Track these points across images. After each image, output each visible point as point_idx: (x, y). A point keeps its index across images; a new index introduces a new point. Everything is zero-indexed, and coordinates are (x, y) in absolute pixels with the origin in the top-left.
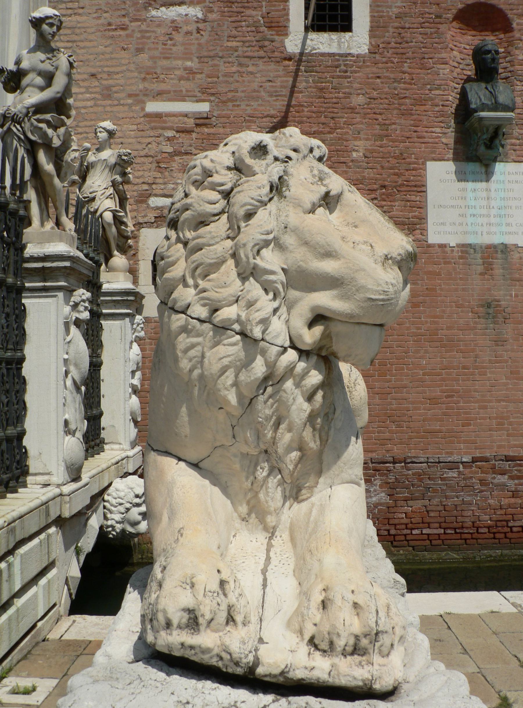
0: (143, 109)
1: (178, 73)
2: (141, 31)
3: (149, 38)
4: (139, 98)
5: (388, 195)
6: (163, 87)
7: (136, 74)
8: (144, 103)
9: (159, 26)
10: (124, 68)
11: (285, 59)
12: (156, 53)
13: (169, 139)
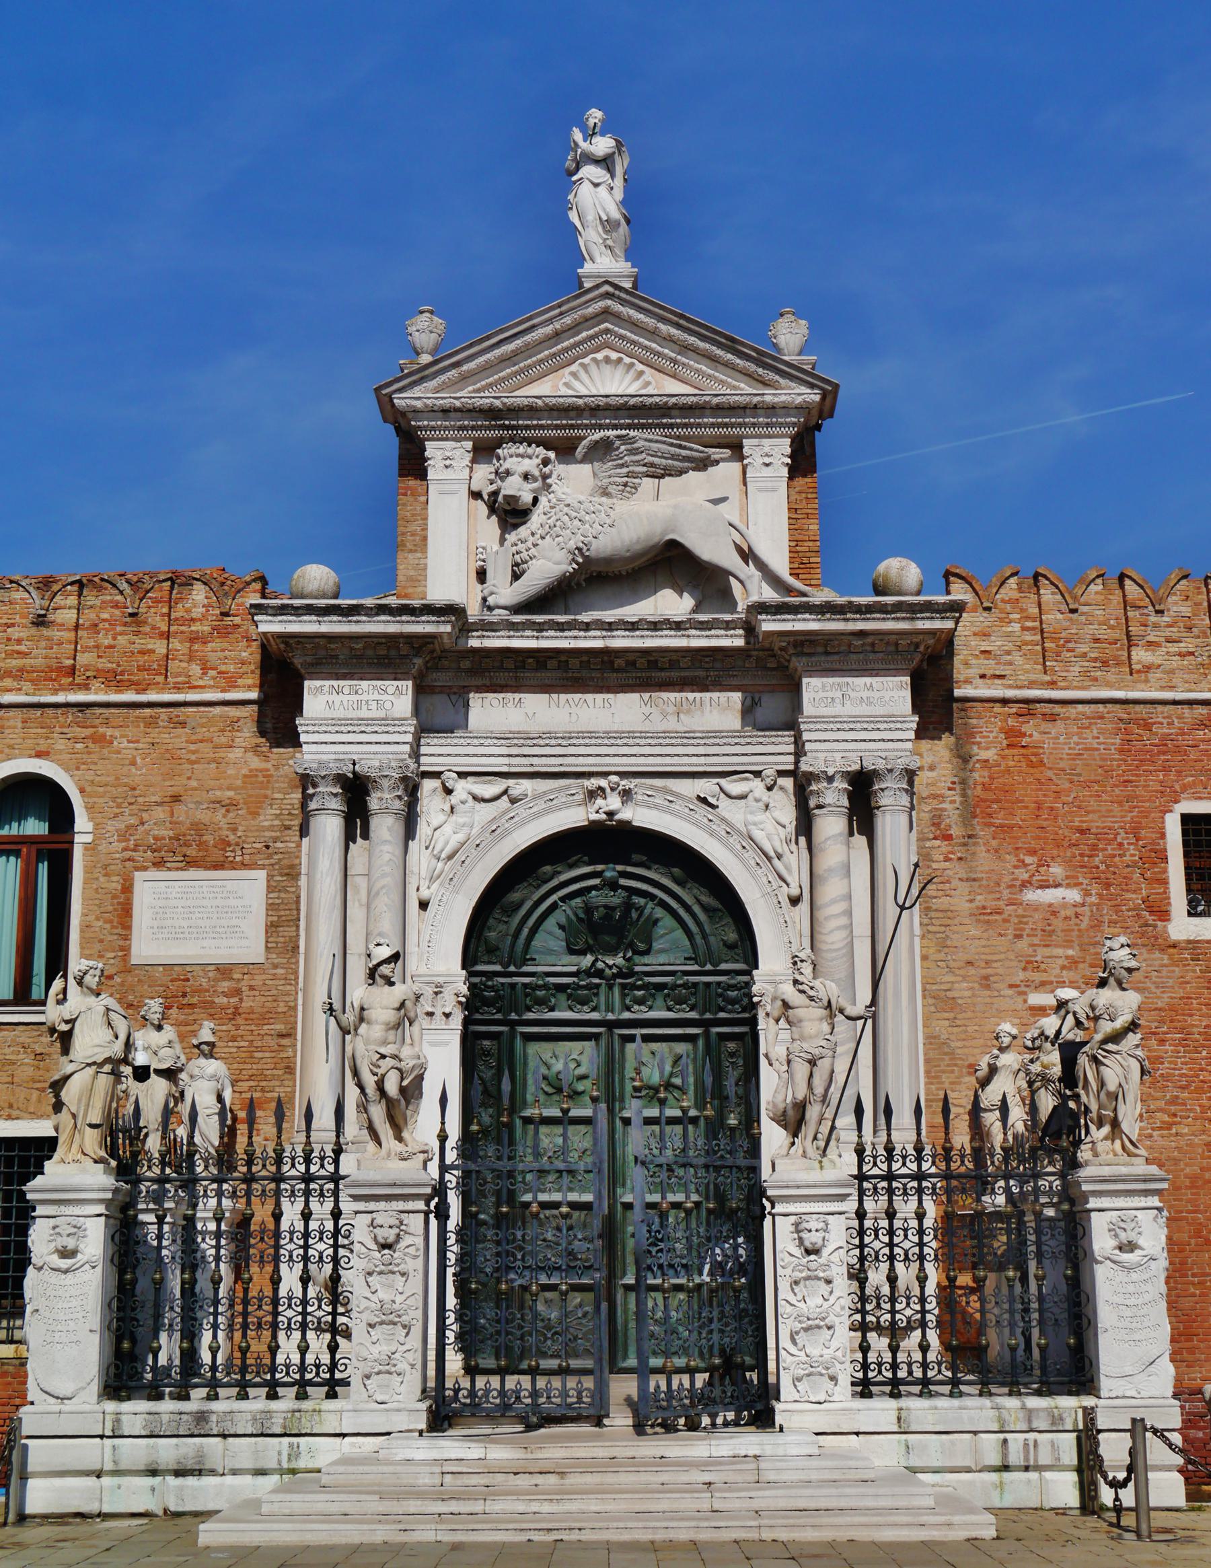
0: (1025, 1001)
1: (1061, 962)
2: (1017, 916)
3: (1026, 923)
7: (1015, 963)
8: (1025, 993)
9: (1036, 910)
10: (1002, 956)
11: (1170, 946)
12: (1036, 941)
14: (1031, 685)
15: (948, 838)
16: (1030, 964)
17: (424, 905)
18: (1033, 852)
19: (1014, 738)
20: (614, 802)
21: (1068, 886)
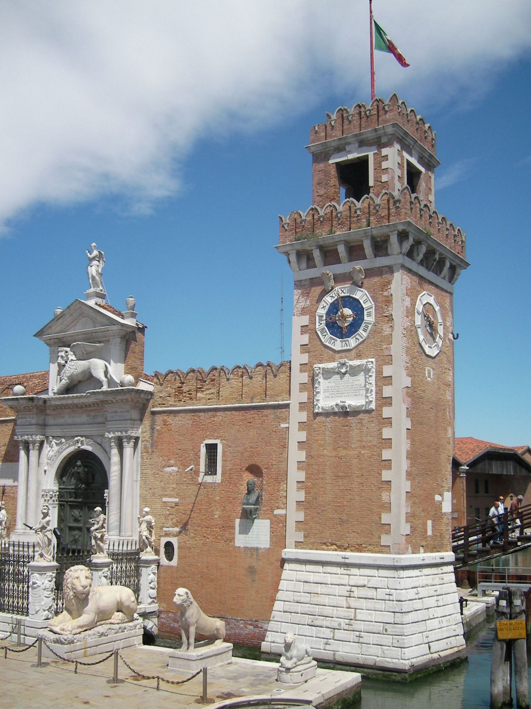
1: (171, 489)
4: (162, 496)
5: (224, 530)
6: (167, 493)
8: (162, 498)
13: (168, 510)
14: (171, 406)
15: (148, 452)
16: (164, 489)
17: (45, 471)
18: (167, 456)
19: (165, 422)
20: (79, 445)
21: (175, 466)
